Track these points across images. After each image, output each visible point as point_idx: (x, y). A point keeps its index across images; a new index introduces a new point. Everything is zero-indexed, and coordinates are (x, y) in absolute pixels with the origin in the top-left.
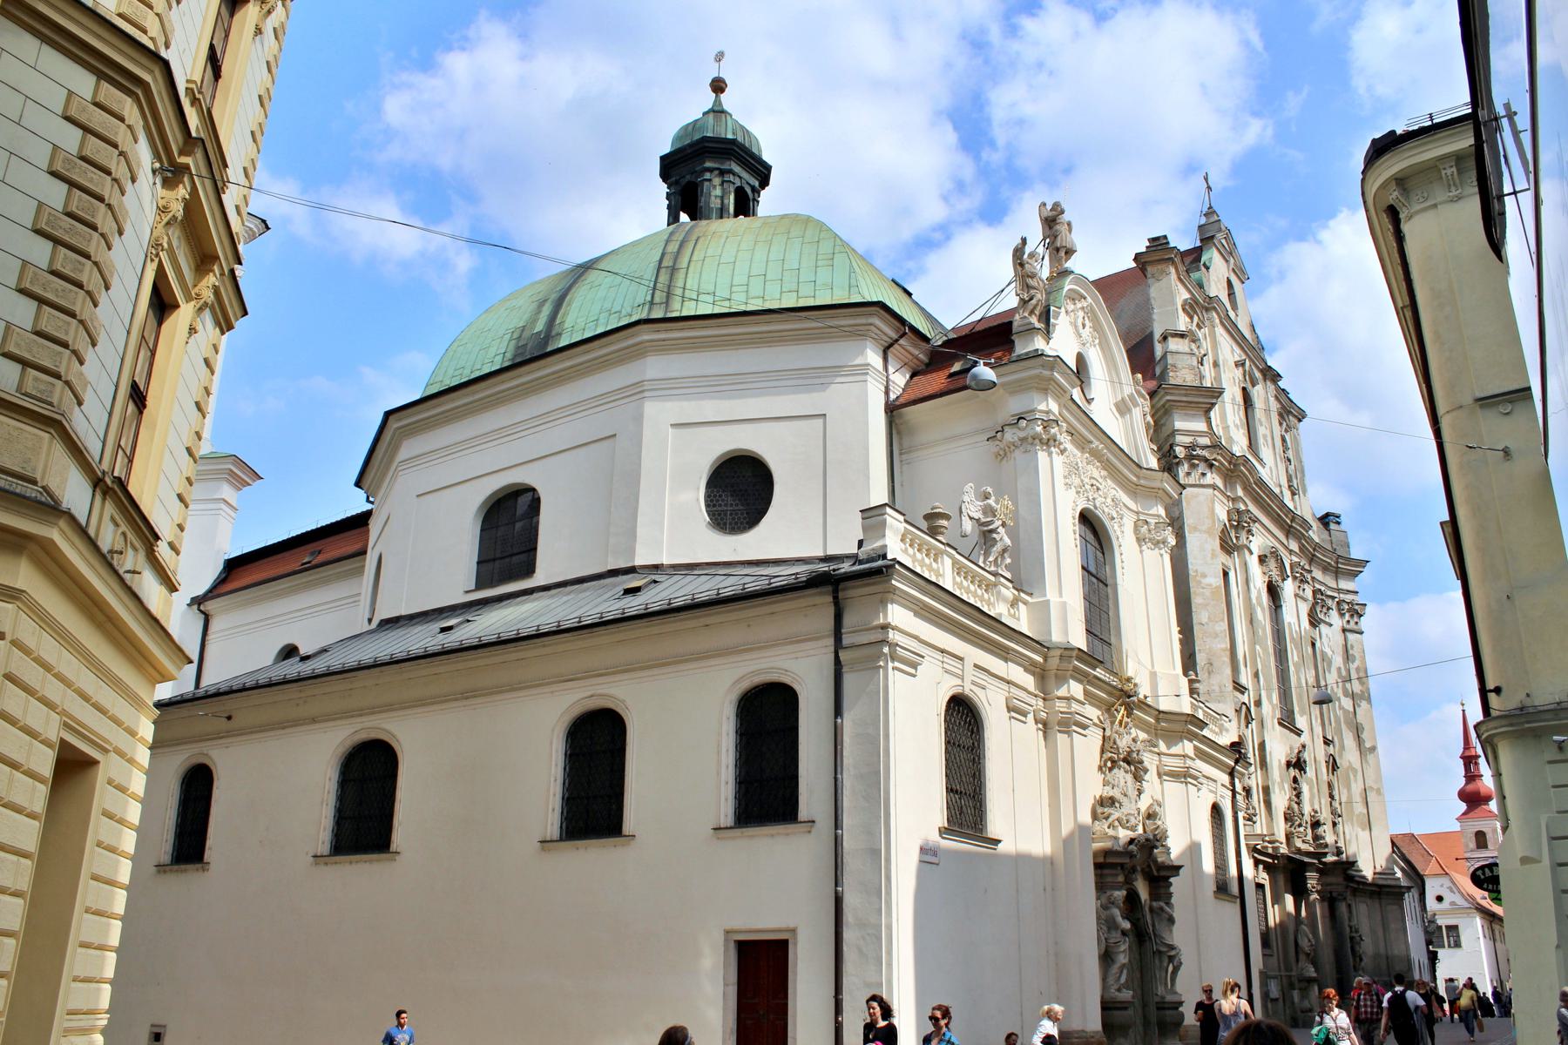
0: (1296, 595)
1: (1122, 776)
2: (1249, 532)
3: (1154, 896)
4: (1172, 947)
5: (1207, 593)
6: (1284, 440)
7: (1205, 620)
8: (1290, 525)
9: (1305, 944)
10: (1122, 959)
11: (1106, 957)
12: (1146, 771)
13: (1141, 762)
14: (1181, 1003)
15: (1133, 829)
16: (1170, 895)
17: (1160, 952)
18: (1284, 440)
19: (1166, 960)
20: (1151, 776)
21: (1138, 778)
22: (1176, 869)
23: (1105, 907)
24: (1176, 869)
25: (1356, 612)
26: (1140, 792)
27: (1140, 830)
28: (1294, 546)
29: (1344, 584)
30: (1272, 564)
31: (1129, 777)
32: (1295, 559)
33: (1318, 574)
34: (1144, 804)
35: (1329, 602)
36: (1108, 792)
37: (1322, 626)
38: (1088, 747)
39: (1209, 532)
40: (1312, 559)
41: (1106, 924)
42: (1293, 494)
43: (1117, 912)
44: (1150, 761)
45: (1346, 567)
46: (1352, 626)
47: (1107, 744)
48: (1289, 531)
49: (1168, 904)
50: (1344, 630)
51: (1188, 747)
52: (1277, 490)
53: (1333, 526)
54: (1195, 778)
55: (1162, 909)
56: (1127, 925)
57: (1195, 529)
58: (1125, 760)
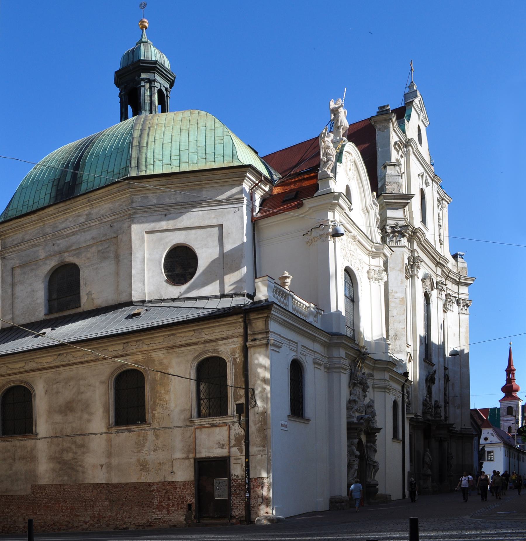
1: (358, 390)
2: (418, 267)
3: (368, 441)
4: (375, 462)
5: (397, 301)
7: (395, 314)
9: (427, 460)
10: (356, 467)
11: (350, 466)
12: (368, 387)
13: (366, 383)
14: (377, 485)
15: (361, 413)
16: (376, 440)
17: (370, 464)
18: (439, 216)
19: (372, 467)
20: (370, 390)
21: (364, 390)
22: (379, 430)
23: (349, 446)
24: (379, 430)
26: (365, 396)
27: (364, 414)
28: (439, 271)
30: (428, 282)
31: (361, 391)
32: (439, 279)
33: (450, 285)
34: (367, 401)
36: (353, 397)
38: (345, 378)
39: (400, 270)
41: (350, 453)
42: (441, 244)
43: (354, 448)
44: (370, 382)
47: (352, 376)
48: (438, 264)
49: (374, 444)
51: (387, 376)
54: (389, 389)
55: (371, 446)
56: (358, 453)
57: (394, 269)
58: (361, 383)
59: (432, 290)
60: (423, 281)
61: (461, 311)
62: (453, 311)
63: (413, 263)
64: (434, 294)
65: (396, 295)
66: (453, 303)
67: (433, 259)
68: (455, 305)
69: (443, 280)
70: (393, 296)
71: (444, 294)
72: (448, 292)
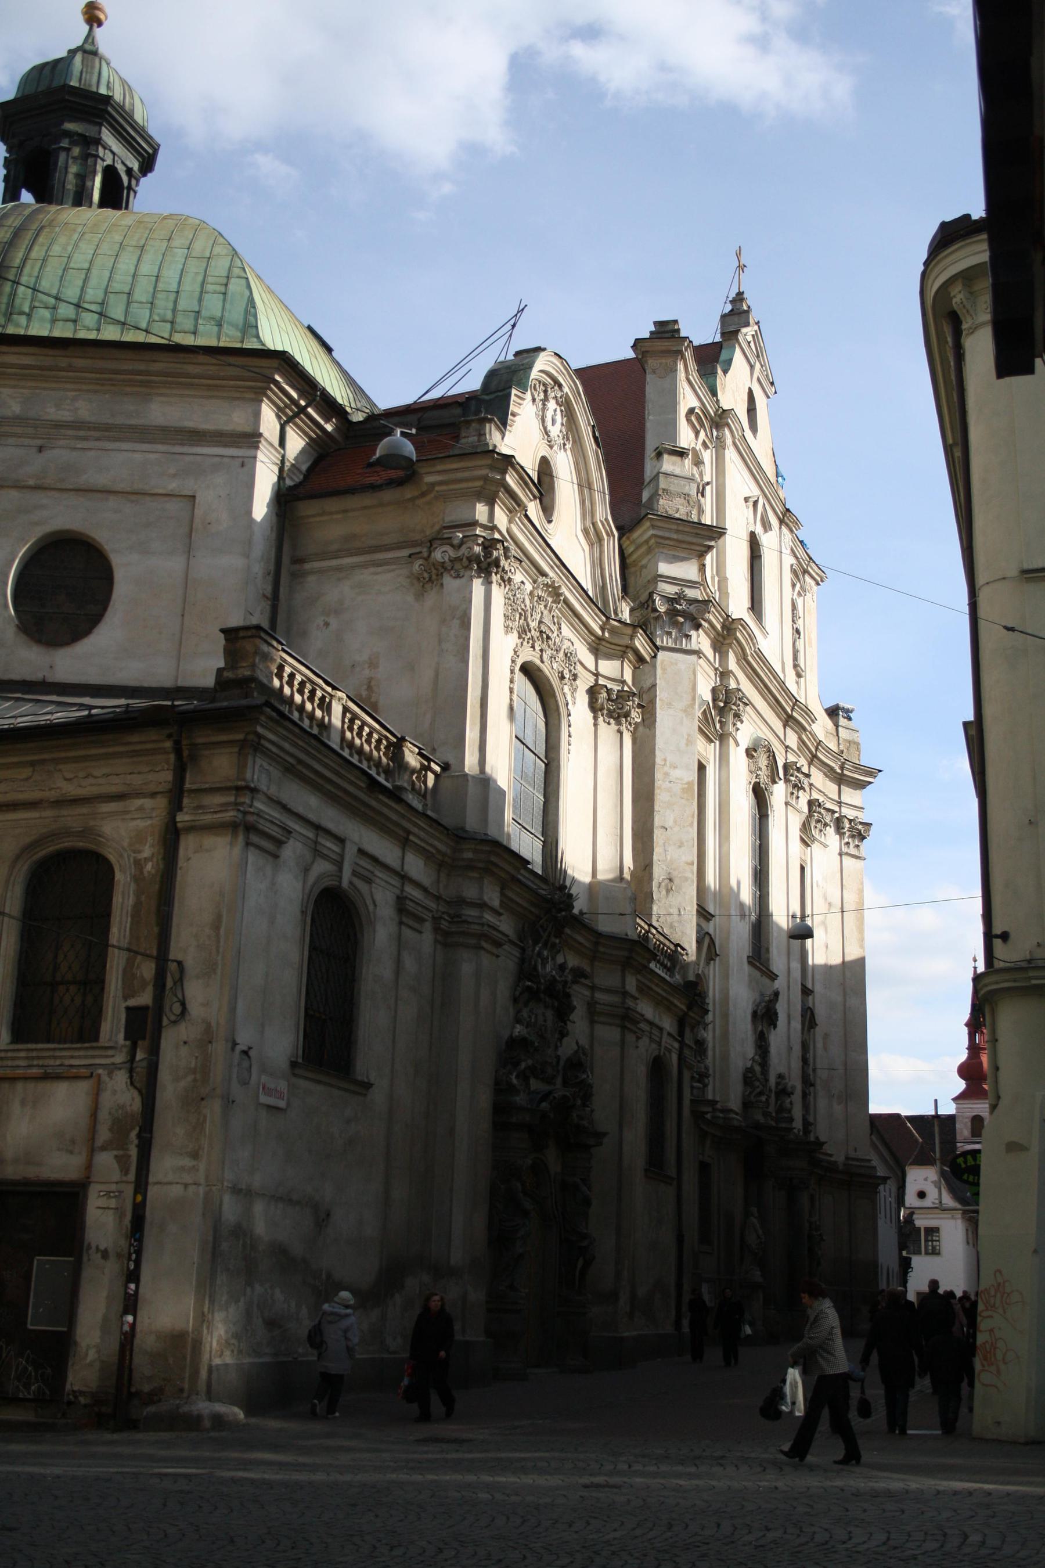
0: (787, 804)
2: (737, 716)
6: (794, 607)
7: (669, 823)
8: (792, 715)
18: (794, 607)
25: (859, 832)
28: (792, 739)
29: (849, 795)
30: (763, 761)
32: (791, 758)
35: (828, 818)
37: (815, 846)
40: (813, 759)
45: (851, 776)
46: (852, 850)
48: (788, 720)
50: (841, 854)
52: (778, 668)
53: (842, 721)
59: (774, 782)
60: (750, 753)
61: (845, 849)
62: (826, 846)
63: (725, 705)
64: (779, 792)
65: (676, 774)
66: (826, 825)
67: (776, 705)
68: (831, 831)
69: (802, 762)
70: (667, 774)
71: (804, 798)
72: (815, 795)
